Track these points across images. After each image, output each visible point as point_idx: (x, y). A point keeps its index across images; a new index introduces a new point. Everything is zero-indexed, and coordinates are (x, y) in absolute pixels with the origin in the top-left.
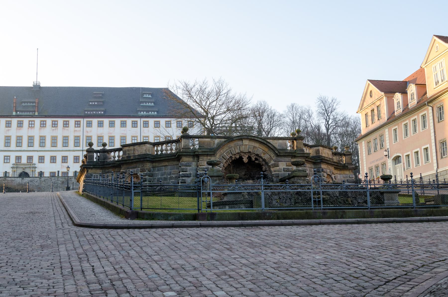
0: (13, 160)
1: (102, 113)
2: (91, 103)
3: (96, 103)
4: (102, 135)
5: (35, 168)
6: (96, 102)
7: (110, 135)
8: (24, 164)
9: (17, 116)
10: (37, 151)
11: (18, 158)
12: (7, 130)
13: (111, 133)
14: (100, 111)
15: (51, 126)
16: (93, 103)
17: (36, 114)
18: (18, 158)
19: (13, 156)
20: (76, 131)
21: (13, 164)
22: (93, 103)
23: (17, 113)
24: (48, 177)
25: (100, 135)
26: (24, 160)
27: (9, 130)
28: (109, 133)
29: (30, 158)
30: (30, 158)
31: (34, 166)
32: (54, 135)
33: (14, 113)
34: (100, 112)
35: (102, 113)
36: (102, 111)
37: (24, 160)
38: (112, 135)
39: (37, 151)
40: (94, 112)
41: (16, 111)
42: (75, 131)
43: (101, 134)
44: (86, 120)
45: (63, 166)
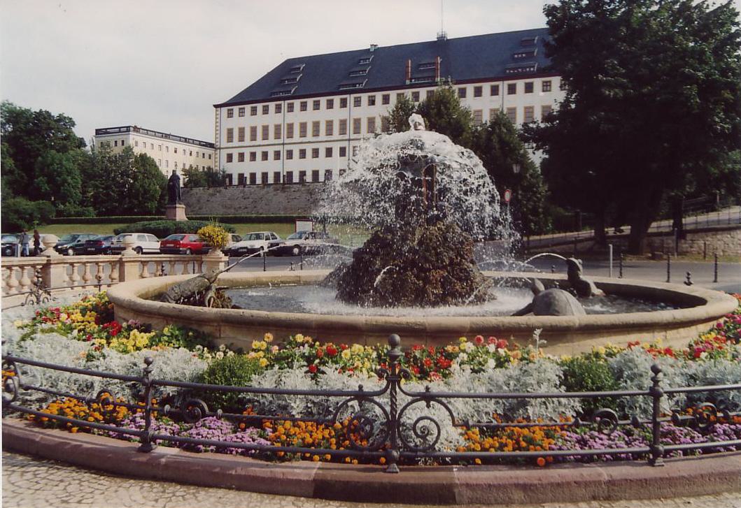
1: (532, 69)
2: (516, 56)
3: (524, 55)
9: (411, 86)
16: (520, 56)
22: (520, 56)
23: (411, 81)
25: (528, 105)
33: (408, 82)
34: (528, 69)
35: (532, 69)
40: (520, 70)
41: (411, 79)
44: (507, 83)
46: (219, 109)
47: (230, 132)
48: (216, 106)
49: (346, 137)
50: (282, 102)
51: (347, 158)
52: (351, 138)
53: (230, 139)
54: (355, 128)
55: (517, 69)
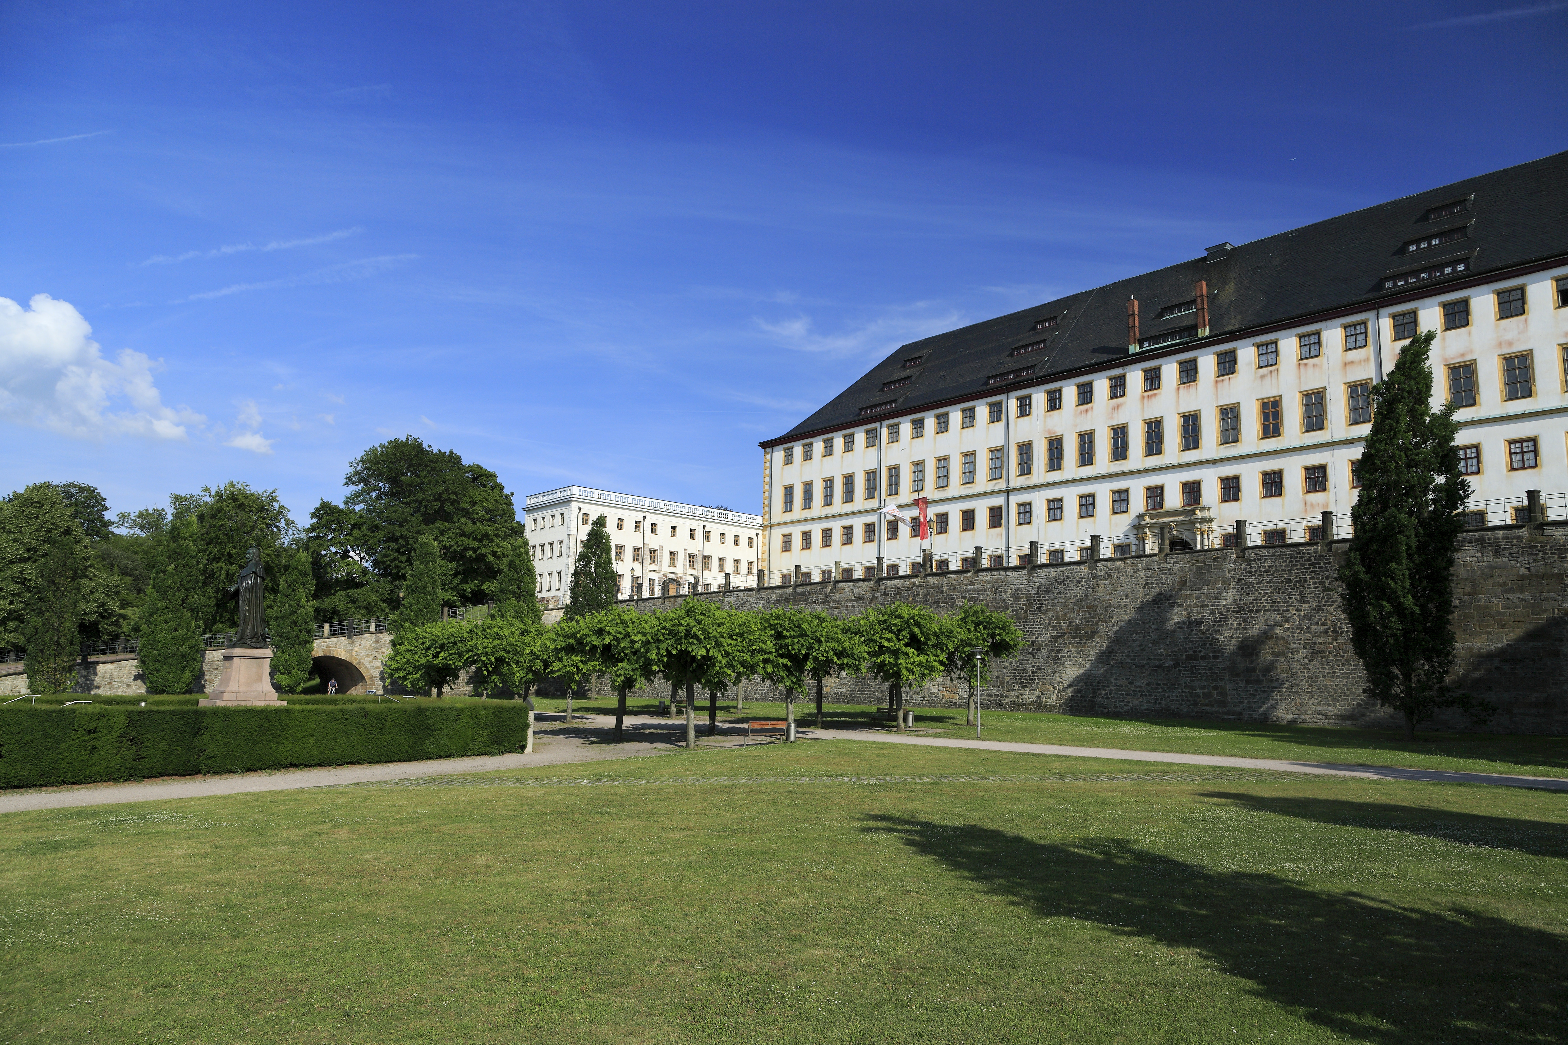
0: (1138, 503)
1: (1461, 267)
3: (1435, 242)
4: (1469, 357)
5: (1210, 520)
6: (1435, 236)
7: (1506, 350)
8: (1173, 513)
9: (1140, 358)
10: (1214, 462)
11: (1156, 494)
12: (1114, 408)
13: (1510, 344)
14: (1448, 265)
15: (1254, 366)
16: (1424, 245)
17: (1204, 332)
18: (1156, 494)
19: (1137, 489)
20: (1352, 362)
21: (1140, 517)
24: (746, 590)
26: (1174, 499)
27: (1118, 406)
28: (1500, 344)
29: (1192, 491)
30: (1192, 491)
31: (1206, 514)
32: (1269, 392)
33: (1134, 349)
34: (1448, 270)
36: (1459, 262)
37: (1174, 499)
38: (1520, 347)
39: (1214, 462)
40: (1425, 275)
42: (1345, 364)
43: (1463, 355)
45: (1312, 505)
46: (769, 450)
47: (789, 491)
48: (768, 445)
49: (1001, 485)
50: (877, 425)
51: (1002, 530)
52: (1013, 485)
53: (788, 505)
54: (1021, 464)
55: (1415, 273)
